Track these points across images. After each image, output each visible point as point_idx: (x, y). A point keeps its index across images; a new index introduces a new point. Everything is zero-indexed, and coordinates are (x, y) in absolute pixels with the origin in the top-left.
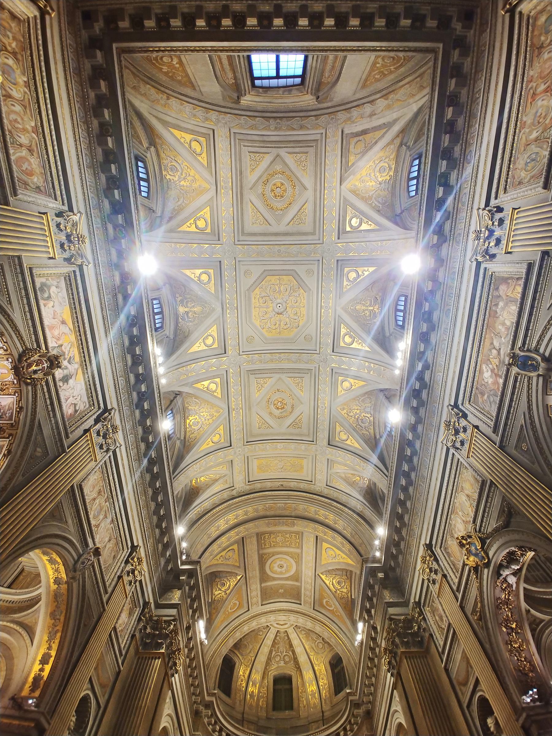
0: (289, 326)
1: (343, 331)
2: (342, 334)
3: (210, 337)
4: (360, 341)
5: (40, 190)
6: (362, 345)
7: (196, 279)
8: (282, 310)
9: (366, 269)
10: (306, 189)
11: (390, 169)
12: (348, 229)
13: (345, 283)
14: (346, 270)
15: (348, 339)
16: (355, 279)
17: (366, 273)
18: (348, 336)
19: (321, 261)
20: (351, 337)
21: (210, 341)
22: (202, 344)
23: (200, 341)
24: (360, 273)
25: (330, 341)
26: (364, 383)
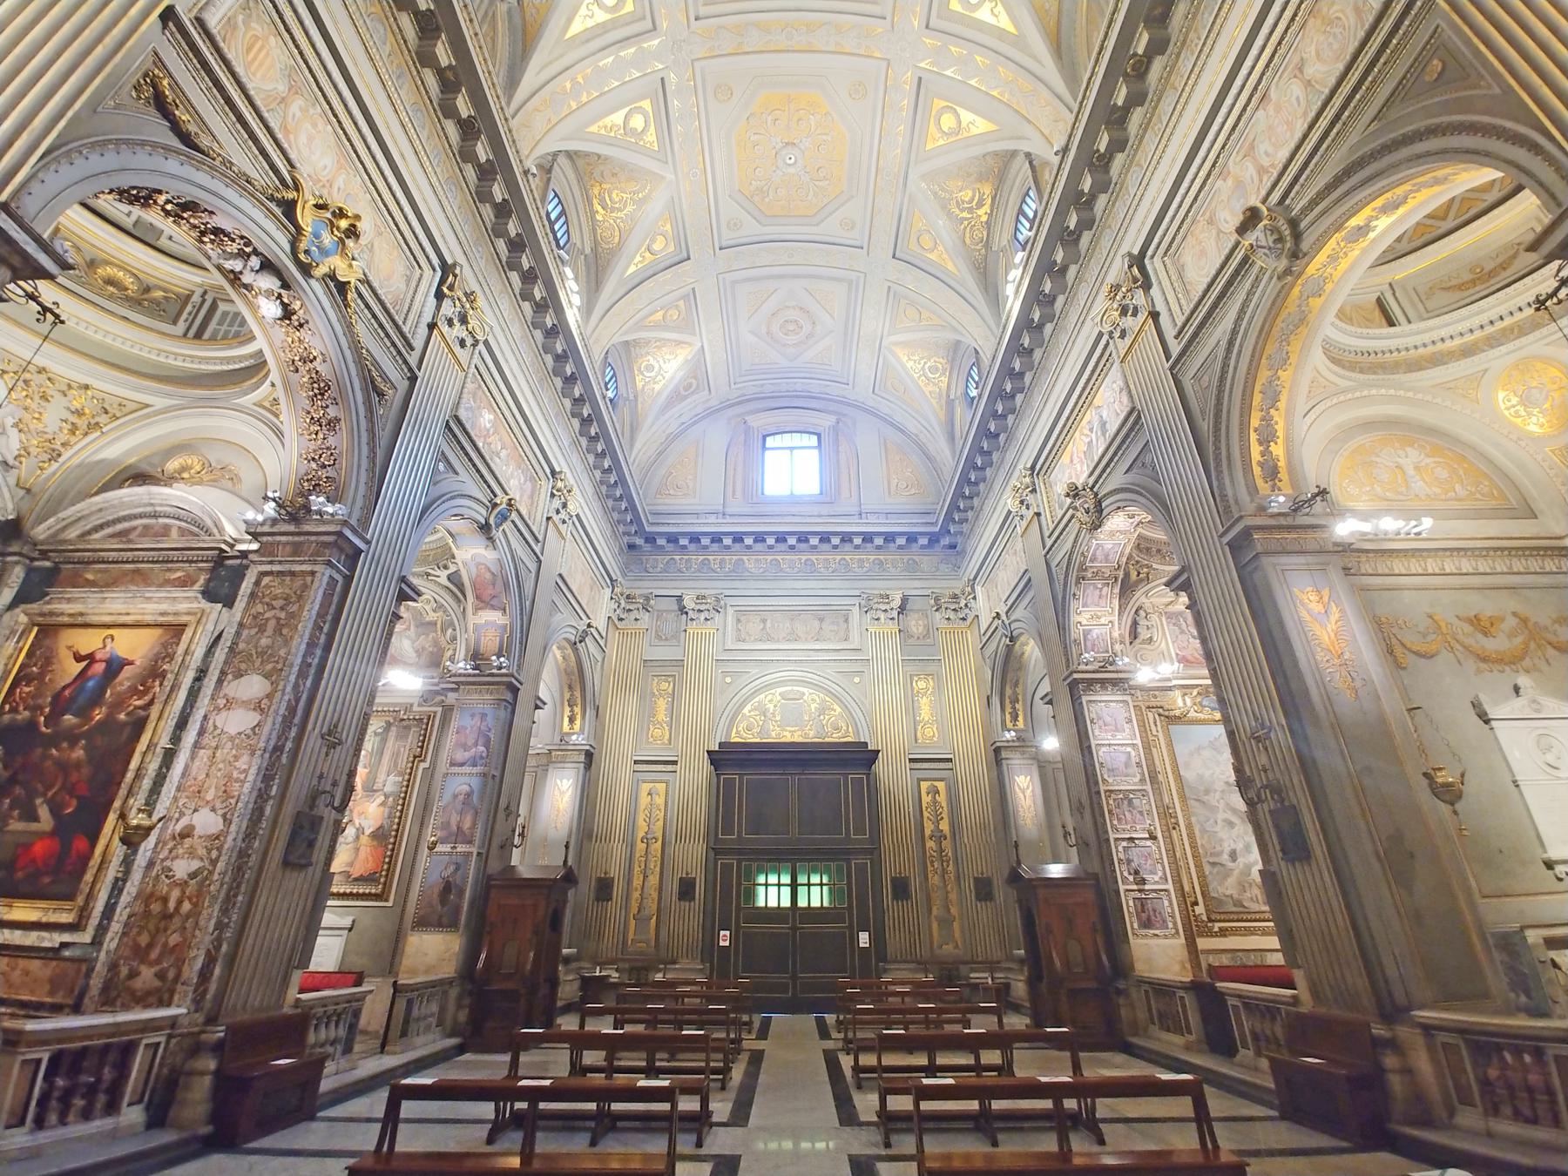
0: (770, 118)
1: (651, 136)
2: (652, 129)
3: (945, 129)
4: (612, 134)
5: (1211, 217)
6: (606, 127)
7: (941, 248)
8: (783, 153)
9: (640, 266)
10: (751, 332)
11: (639, 370)
12: (681, 303)
13: (668, 227)
14: (672, 248)
15: (637, 122)
16: (653, 241)
17: (638, 258)
18: (640, 130)
19: (692, 18)
20: (633, 131)
21: (948, 121)
22: (964, 124)
23: (965, 135)
24: (647, 254)
25: (675, 103)
26: (569, 35)
